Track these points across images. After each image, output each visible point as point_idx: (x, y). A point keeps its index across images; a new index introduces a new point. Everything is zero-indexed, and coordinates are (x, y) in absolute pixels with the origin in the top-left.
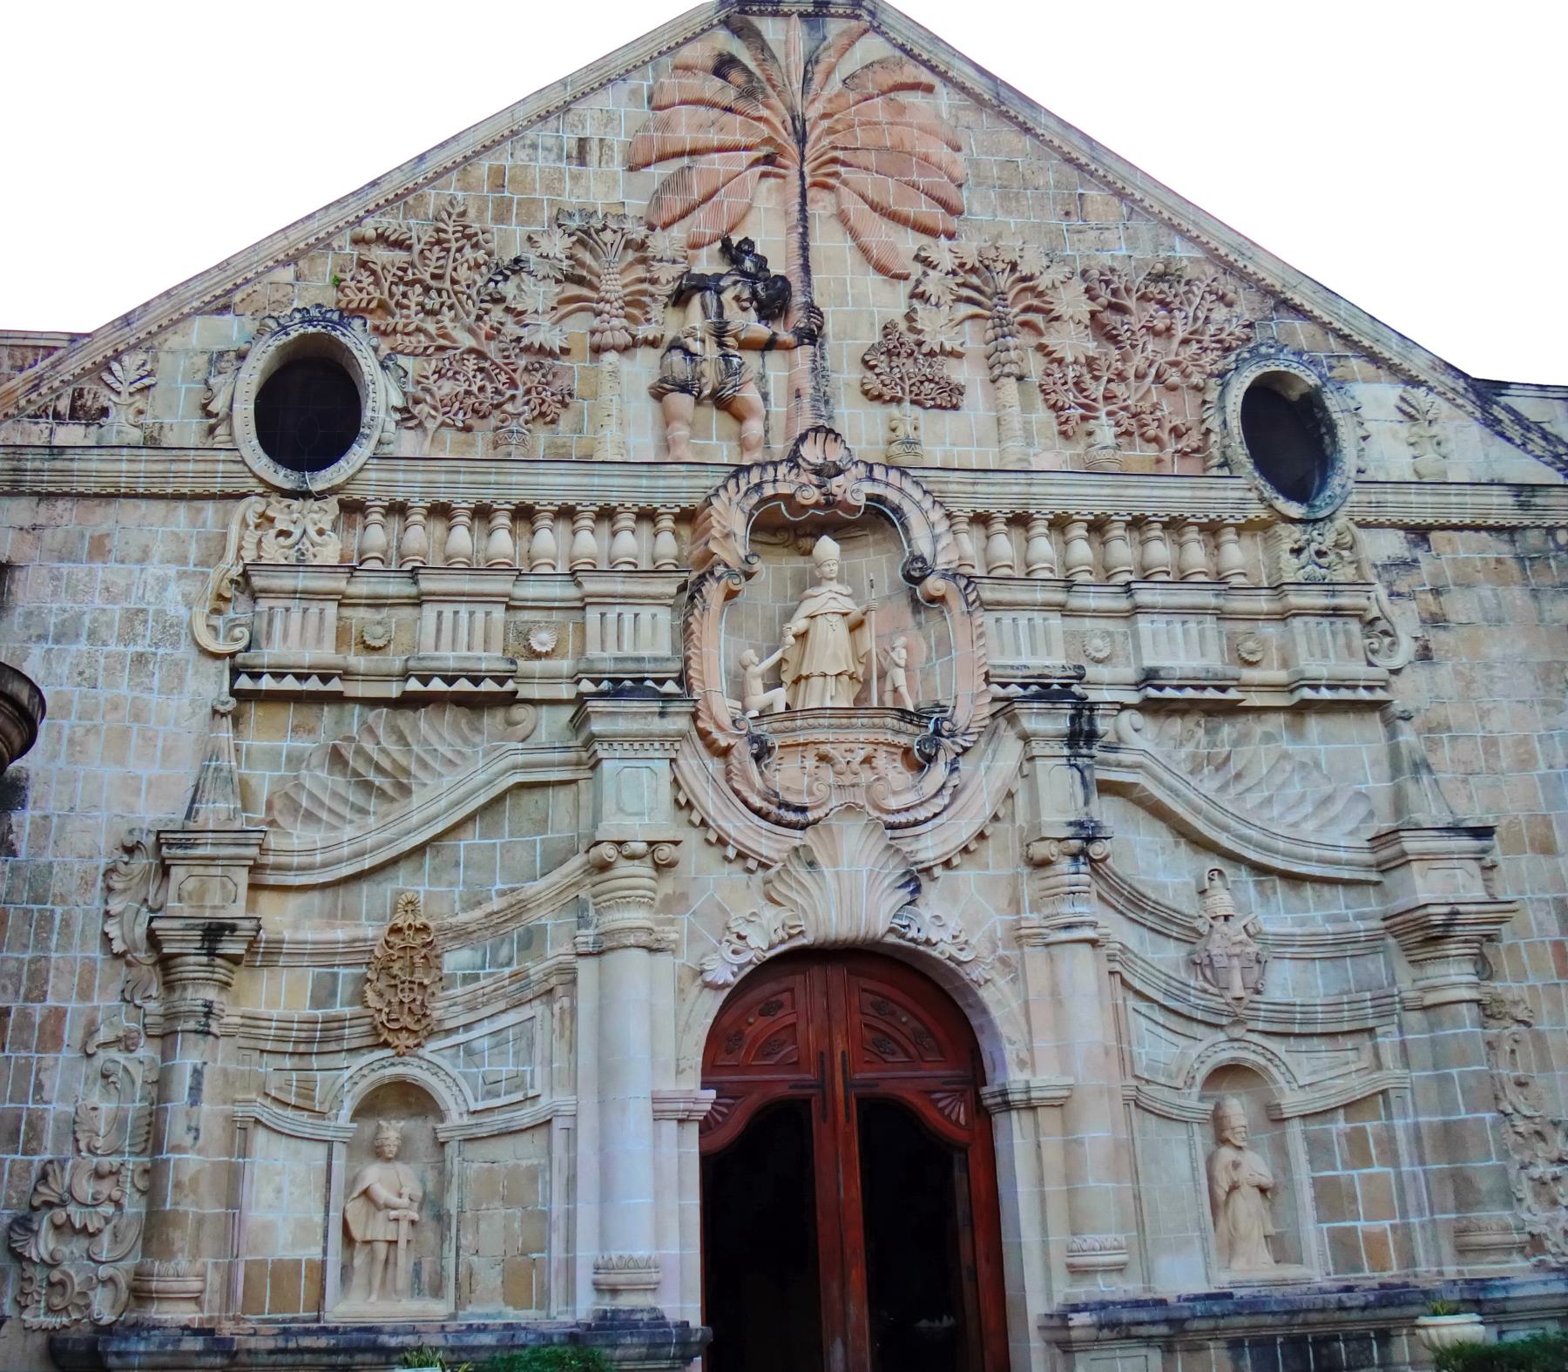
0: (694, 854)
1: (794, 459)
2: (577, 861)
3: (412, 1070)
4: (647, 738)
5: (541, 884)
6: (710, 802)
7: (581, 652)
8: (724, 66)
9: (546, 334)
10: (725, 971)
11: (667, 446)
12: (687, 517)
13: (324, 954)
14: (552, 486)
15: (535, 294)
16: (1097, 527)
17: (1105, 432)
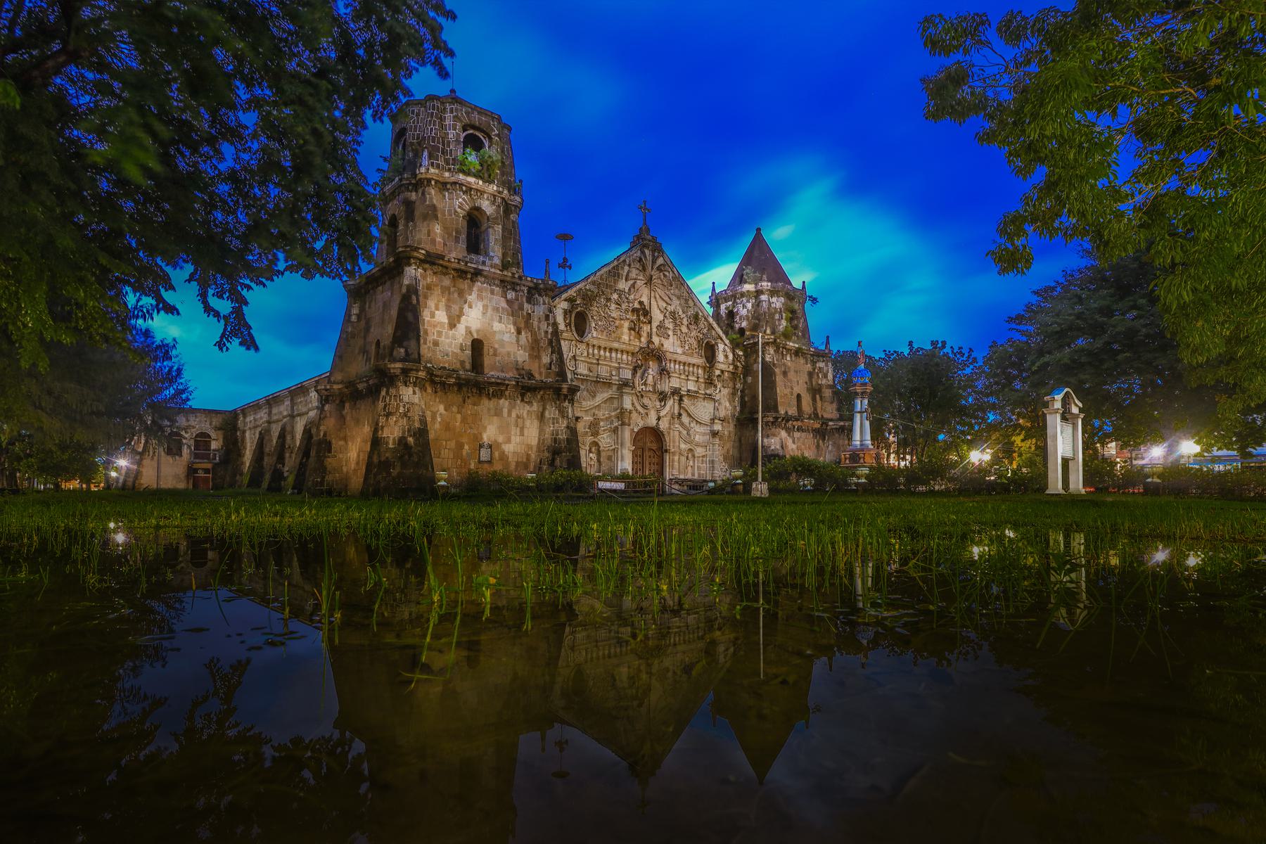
0: (634, 412)
1: (648, 347)
2: (619, 411)
3: (596, 440)
4: (630, 393)
5: (613, 414)
6: (636, 404)
7: (619, 376)
8: (640, 260)
9: (614, 315)
10: (636, 430)
11: (630, 340)
12: (633, 354)
13: (585, 421)
14: (616, 345)
15: (613, 306)
16: (684, 364)
17: (687, 348)
